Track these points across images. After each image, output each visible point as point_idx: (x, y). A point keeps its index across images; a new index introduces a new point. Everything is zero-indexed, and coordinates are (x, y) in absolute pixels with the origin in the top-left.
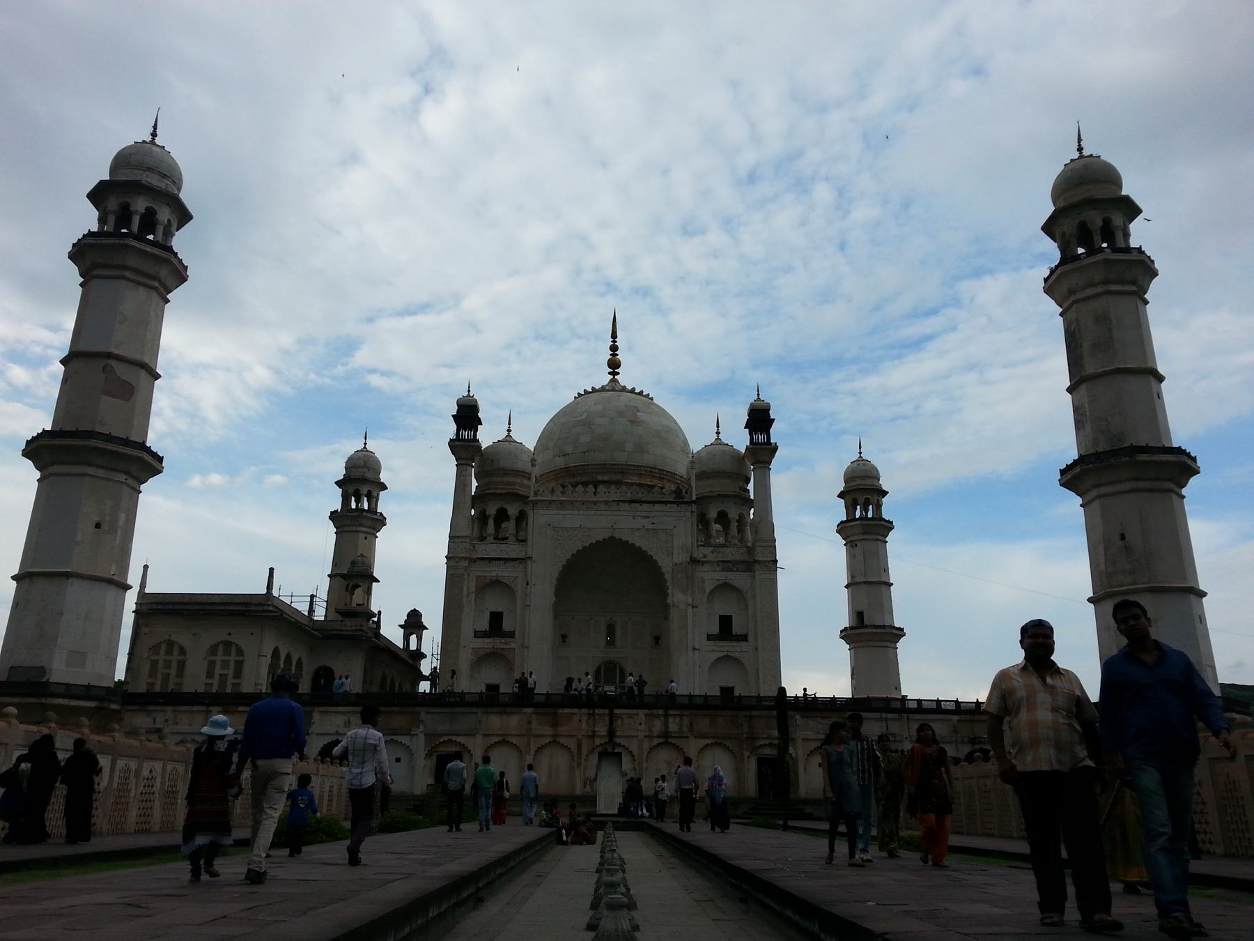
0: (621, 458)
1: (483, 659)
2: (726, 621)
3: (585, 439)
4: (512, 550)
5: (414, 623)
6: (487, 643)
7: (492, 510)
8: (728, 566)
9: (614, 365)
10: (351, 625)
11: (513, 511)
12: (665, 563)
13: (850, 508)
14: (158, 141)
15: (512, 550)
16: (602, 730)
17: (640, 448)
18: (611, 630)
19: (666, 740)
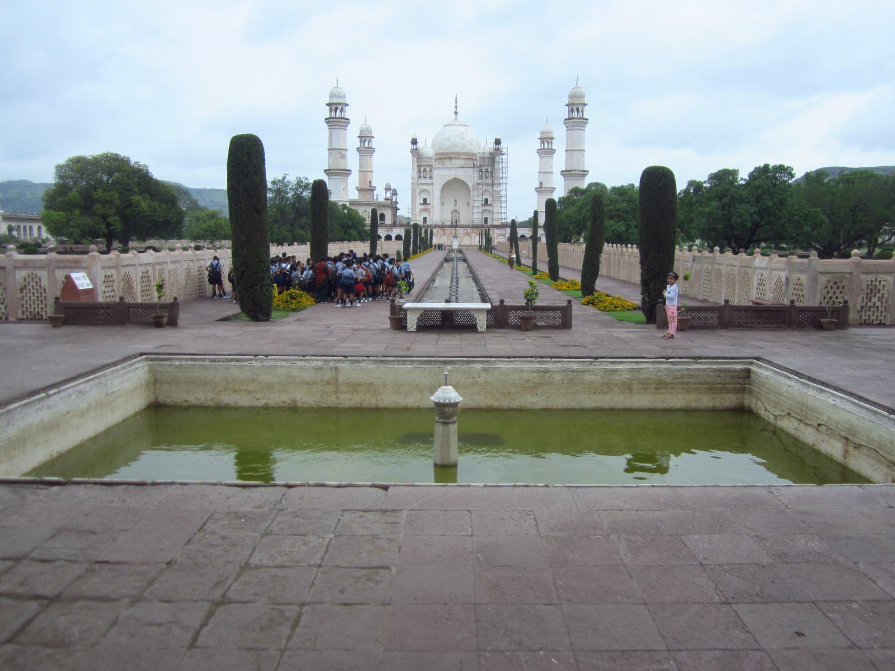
0: (458, 150)
1: (422, 211)
2: (486, 200)
3: (448, 144)
4: (429, 181)
5: (395, 193)
6: (423, 207)
7: (422, 169)
8: (487, 185)
9: (456, 113)
10: (388, 202)
11: (428, 169)
12: (470, 185)
13: (543, 142)
14: (340, 86)
15: (429, 181)
16: (454, 232)
17: (464, 147)
18: (456, 201)
19: (467, 234)
